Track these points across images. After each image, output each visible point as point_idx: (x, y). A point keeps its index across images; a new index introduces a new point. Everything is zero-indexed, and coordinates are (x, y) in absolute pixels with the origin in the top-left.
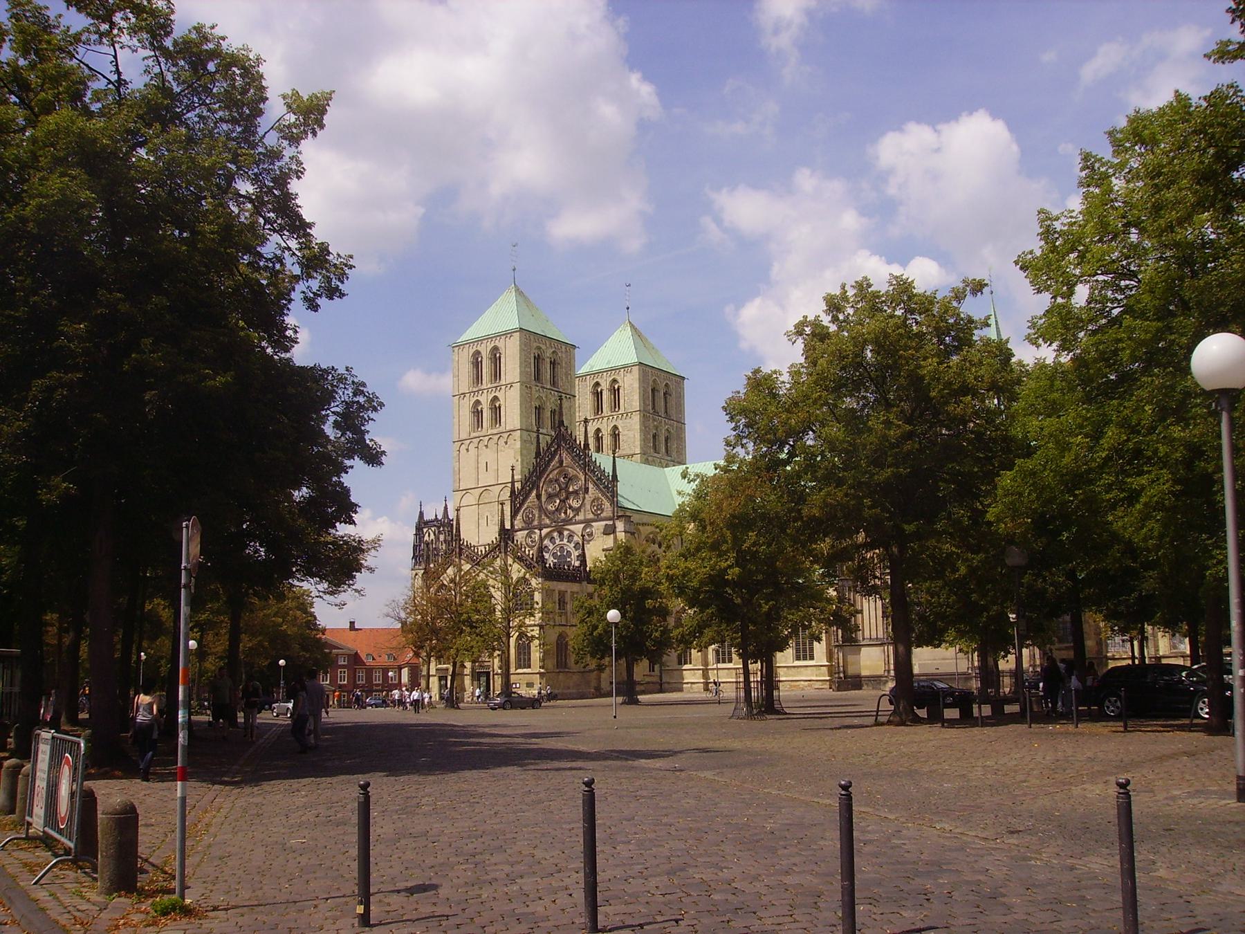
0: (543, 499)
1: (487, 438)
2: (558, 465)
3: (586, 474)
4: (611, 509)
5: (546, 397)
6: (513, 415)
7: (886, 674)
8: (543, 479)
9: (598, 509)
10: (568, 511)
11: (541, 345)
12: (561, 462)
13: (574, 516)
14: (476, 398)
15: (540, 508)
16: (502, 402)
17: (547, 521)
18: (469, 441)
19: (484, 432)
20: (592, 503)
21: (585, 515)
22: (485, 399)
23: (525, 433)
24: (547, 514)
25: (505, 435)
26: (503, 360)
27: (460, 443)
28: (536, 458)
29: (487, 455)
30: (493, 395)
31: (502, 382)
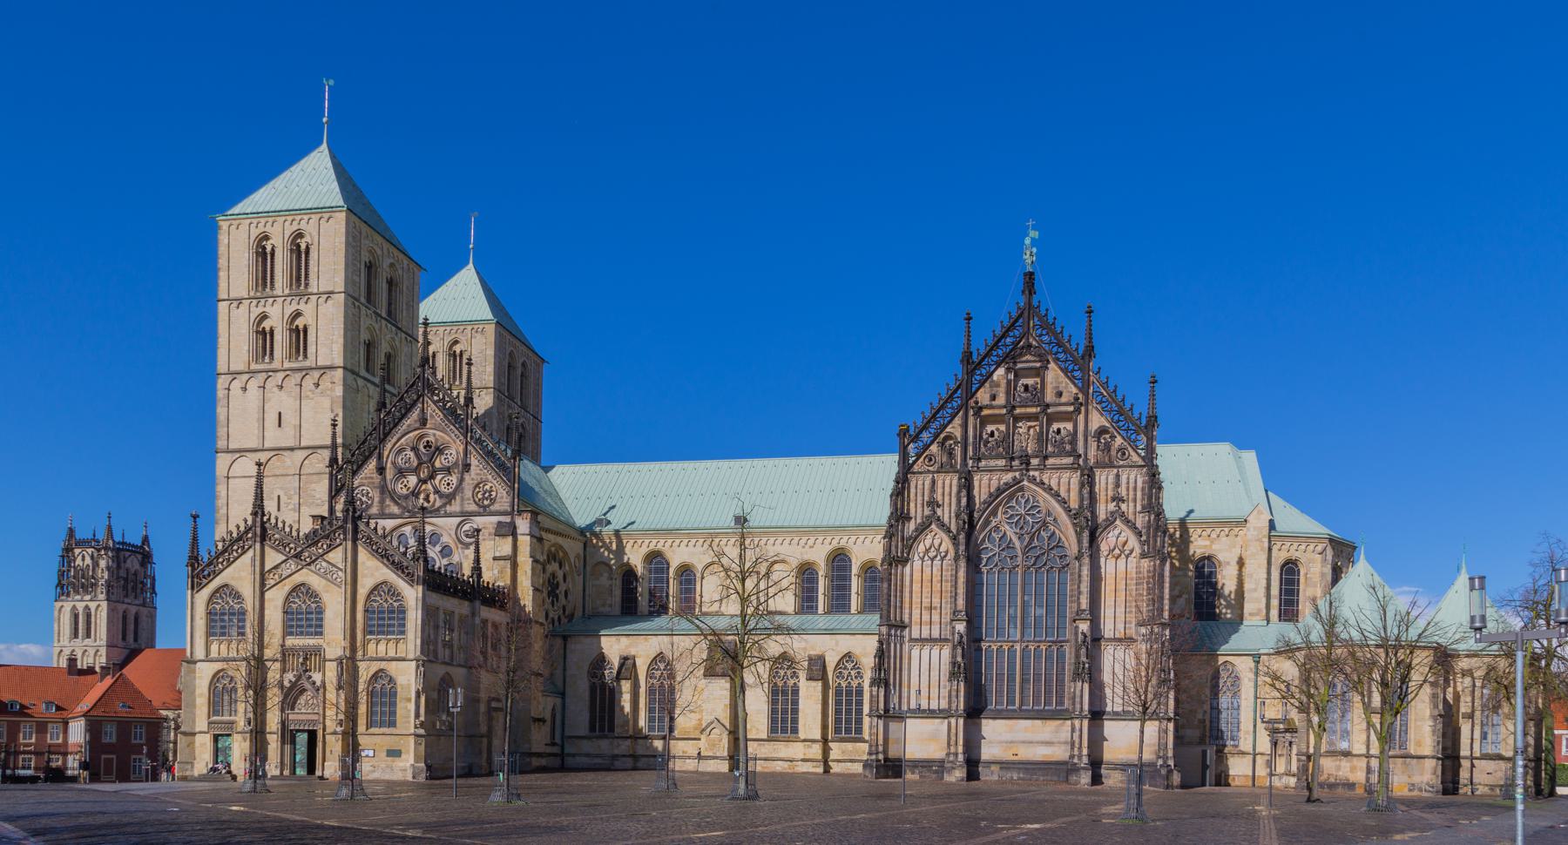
0: (390, 473)
1: (282, 375)
2: (417, 425)
4: (509, 499)
6: (329, 344)
8: (389, 446)
9: (484, 498)
10: (432, 497)
13: (444, 505)
15: (383, 489)
17: (395, 510)
18: (247, 376)
19: (276, 365)
20: (475, 488)
21: (462, 505)
23: (351, 377)
24: (395, 498)
25: (316, 374)
27: (230, 377)
28: (379, 410)
29: (281, 401)
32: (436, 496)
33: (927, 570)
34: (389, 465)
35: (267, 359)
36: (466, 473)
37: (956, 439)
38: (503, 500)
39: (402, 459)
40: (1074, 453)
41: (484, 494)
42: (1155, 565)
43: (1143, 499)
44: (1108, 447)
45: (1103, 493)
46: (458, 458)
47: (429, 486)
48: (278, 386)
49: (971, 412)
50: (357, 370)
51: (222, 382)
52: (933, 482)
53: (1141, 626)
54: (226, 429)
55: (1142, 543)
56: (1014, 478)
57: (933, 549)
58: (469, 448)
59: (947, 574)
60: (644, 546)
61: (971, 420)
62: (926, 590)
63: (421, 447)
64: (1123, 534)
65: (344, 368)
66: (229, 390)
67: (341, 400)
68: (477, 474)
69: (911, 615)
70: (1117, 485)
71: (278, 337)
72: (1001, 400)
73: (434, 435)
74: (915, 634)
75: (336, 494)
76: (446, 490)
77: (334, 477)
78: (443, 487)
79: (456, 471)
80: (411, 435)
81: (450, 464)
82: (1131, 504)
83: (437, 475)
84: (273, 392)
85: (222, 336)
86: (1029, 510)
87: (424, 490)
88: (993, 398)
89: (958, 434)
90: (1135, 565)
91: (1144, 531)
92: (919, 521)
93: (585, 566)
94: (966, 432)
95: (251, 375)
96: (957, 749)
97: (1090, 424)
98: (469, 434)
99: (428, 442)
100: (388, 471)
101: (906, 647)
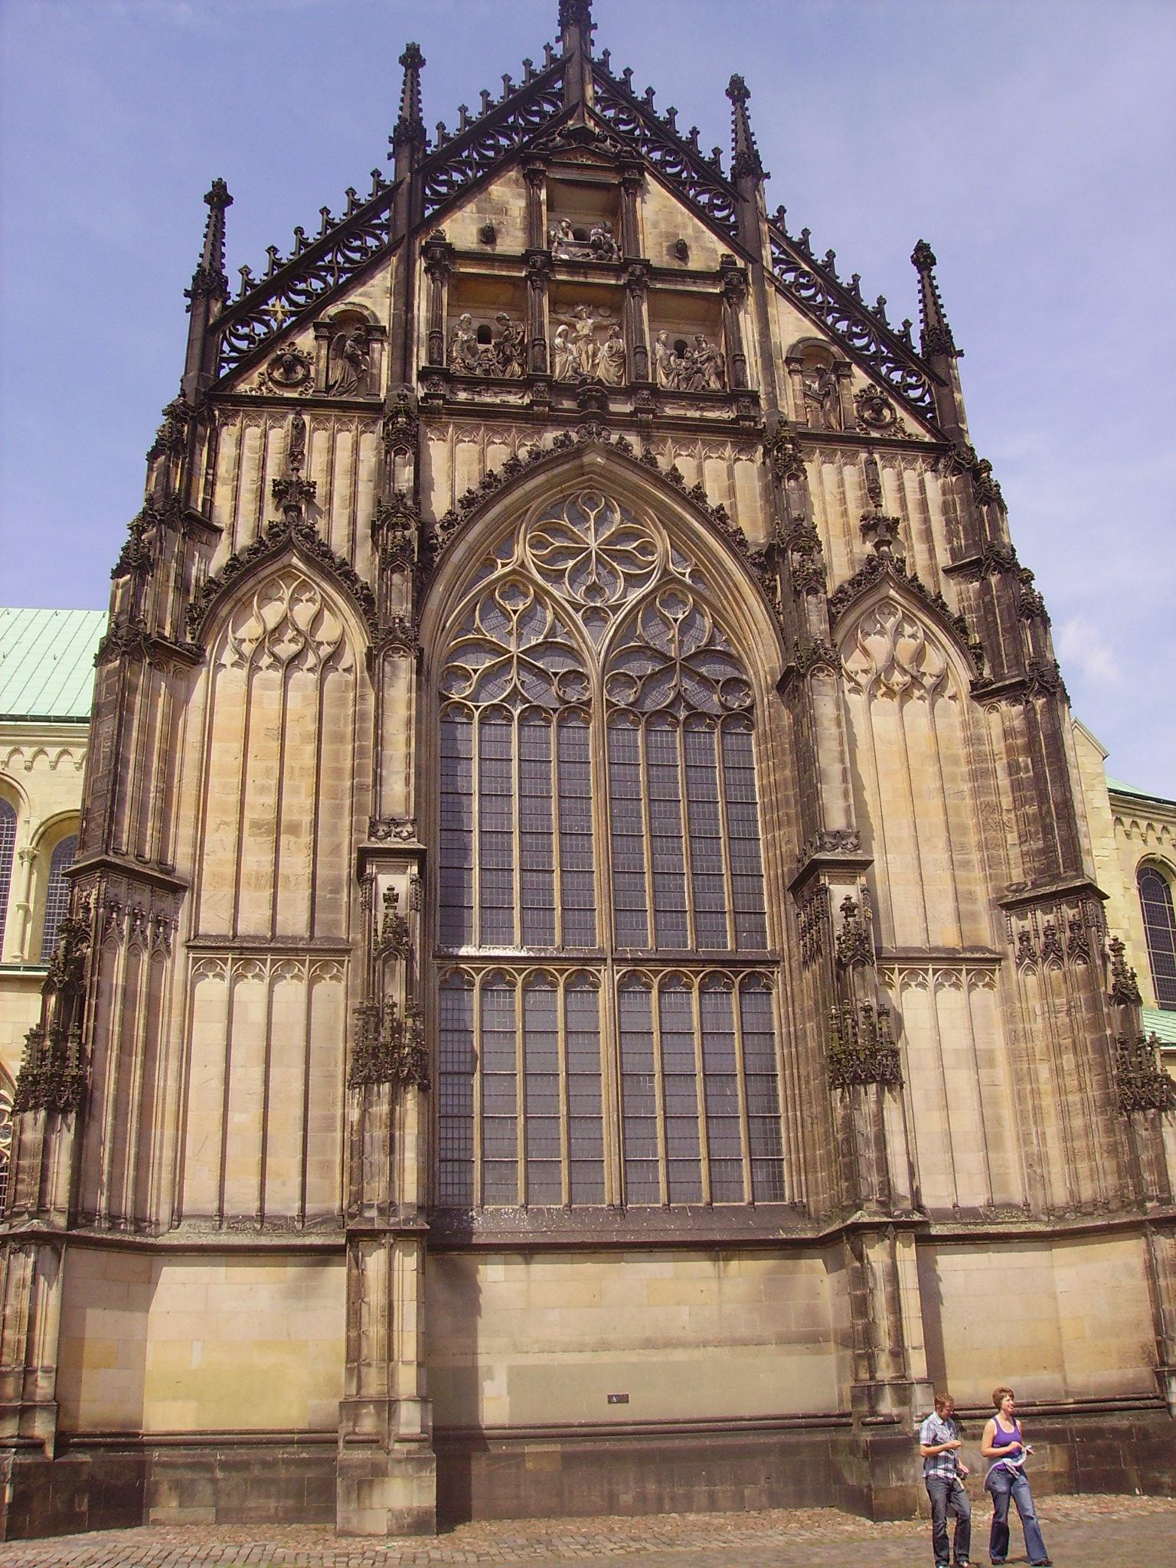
7: (368, 1424)
33: (267, 700)
37: (376, 319)
40: (738, 395)
42: (1029, 714)
43: (951, 535)
44: (829, 394)
45: (834, 510)
49: (421, 264)
52: (299, 429)
53: (1008, 907)
55: (975, 655)
56: (560, 443)
57: (290, 633)
59: (340, 716)
61: (422, 283)
62: (261, 767)
64: (908, 630)
69: (199, 846)
70: (874, 492)
72: (512, 243)
74: (214, 921)
82: (919, 548)
86: (607, 542)
88: (489, 235)
89: (382, 311)
90: (957, 720)
91: (970, 619)
92: (244, 539)
94: (409, 306)
96: (391, 1377)
97: (774, 328)
101: (178, 963)
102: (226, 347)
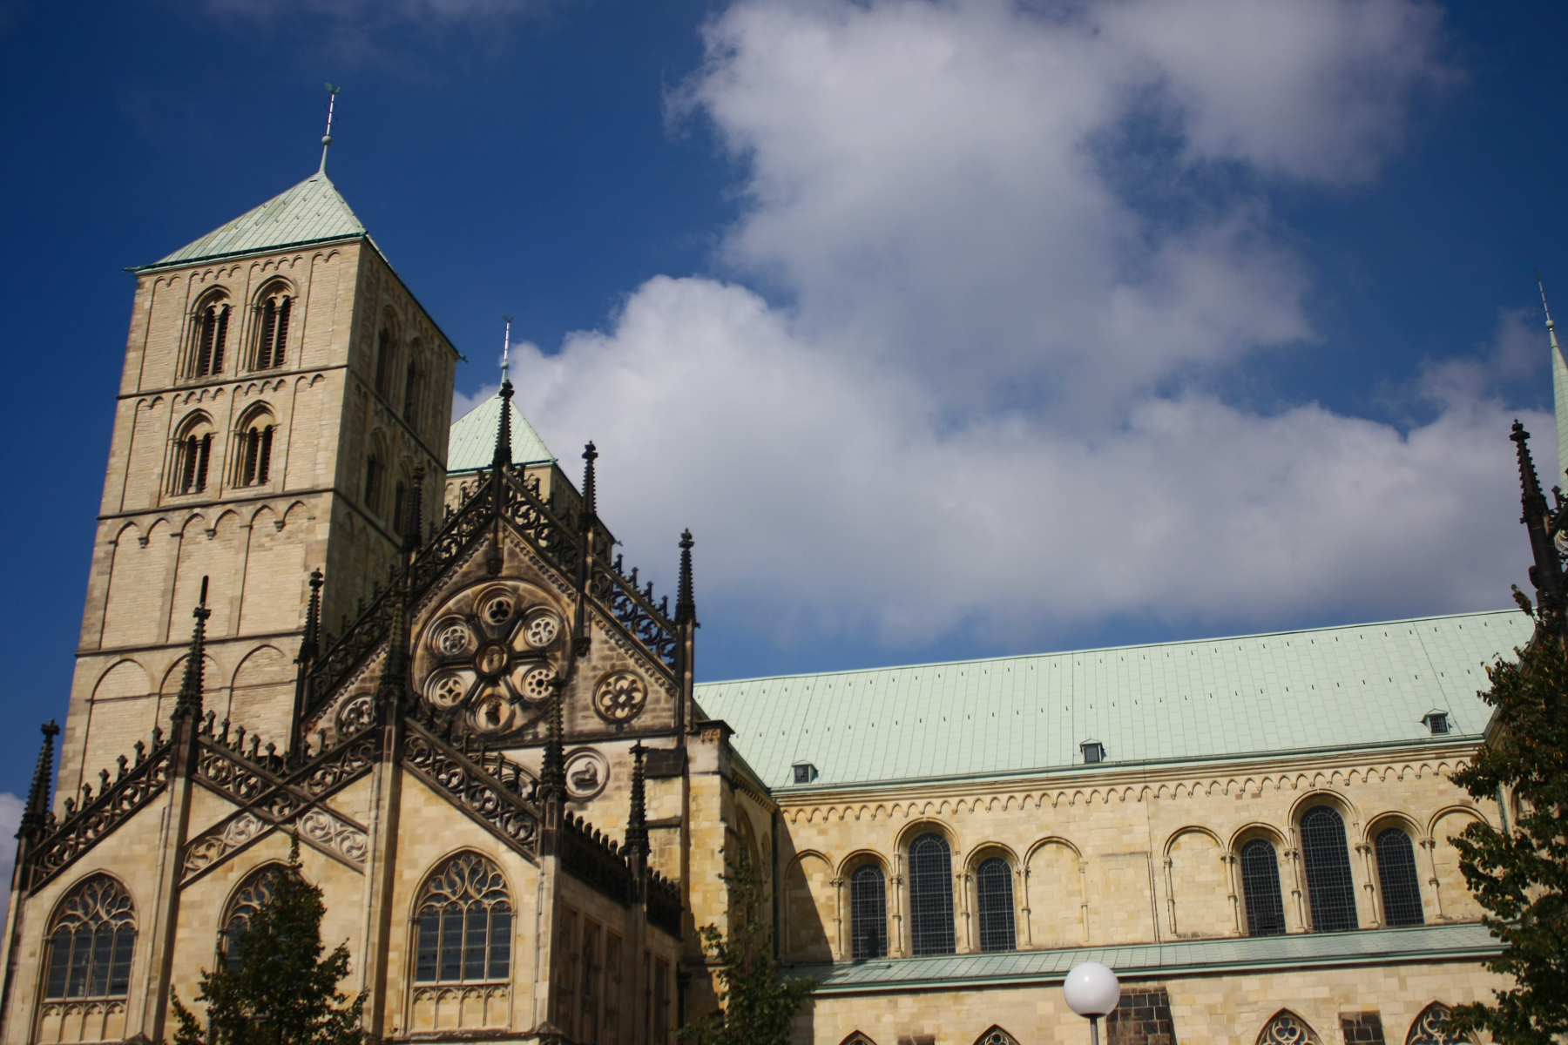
0: (418, 670)
3: (584, 596)
5: (394, 438)
8: (423, 614)
9: (616, 704)
10: (505, 710)
11: (397, 309)
12: (493, 565)
14: (192, 406)
16: (280, 416)
18: (151, 519)
19: (209, 495)
20: (598, 685)
22: (222, 410)
23: (343, 510)
25: (281, 506)
26: (297, 312)
27: (121, 522)
30: (254, 397)
31: (292, 362)
32: (517, 707)
34: (420, 651)
35: (192, 490)
36: (579, 658)
38: (659, 707)
39: (446, 640)
41: (615, 699)
46: (562, 632)
47: (503, 690)
48: (208, 531)
50: (353, 500)
51: (105, 531)
54: (102, 612)
58: (588, 608)
60: (898, 814)
63: (486, 615)
65: (335, 491)
66: (115, 543)
67: (325, 547)
68: (605, 658)
71: (218, 450)
73: (515, 590)
75: (307, 715)
76: (535, 695)
77: (307, 681)
78: (529, 689)
79: (559, 654)
80: (468, 592)
81: (545, 644)
83: (517, 665)
84: (199, 543)
85: (117, 453)
87: (491, 696)
93: (775, 860)
95: (161, 515)
98: (589, 583)
99: (500, 604)
100: (417, 664)
102: (1559, 549)
